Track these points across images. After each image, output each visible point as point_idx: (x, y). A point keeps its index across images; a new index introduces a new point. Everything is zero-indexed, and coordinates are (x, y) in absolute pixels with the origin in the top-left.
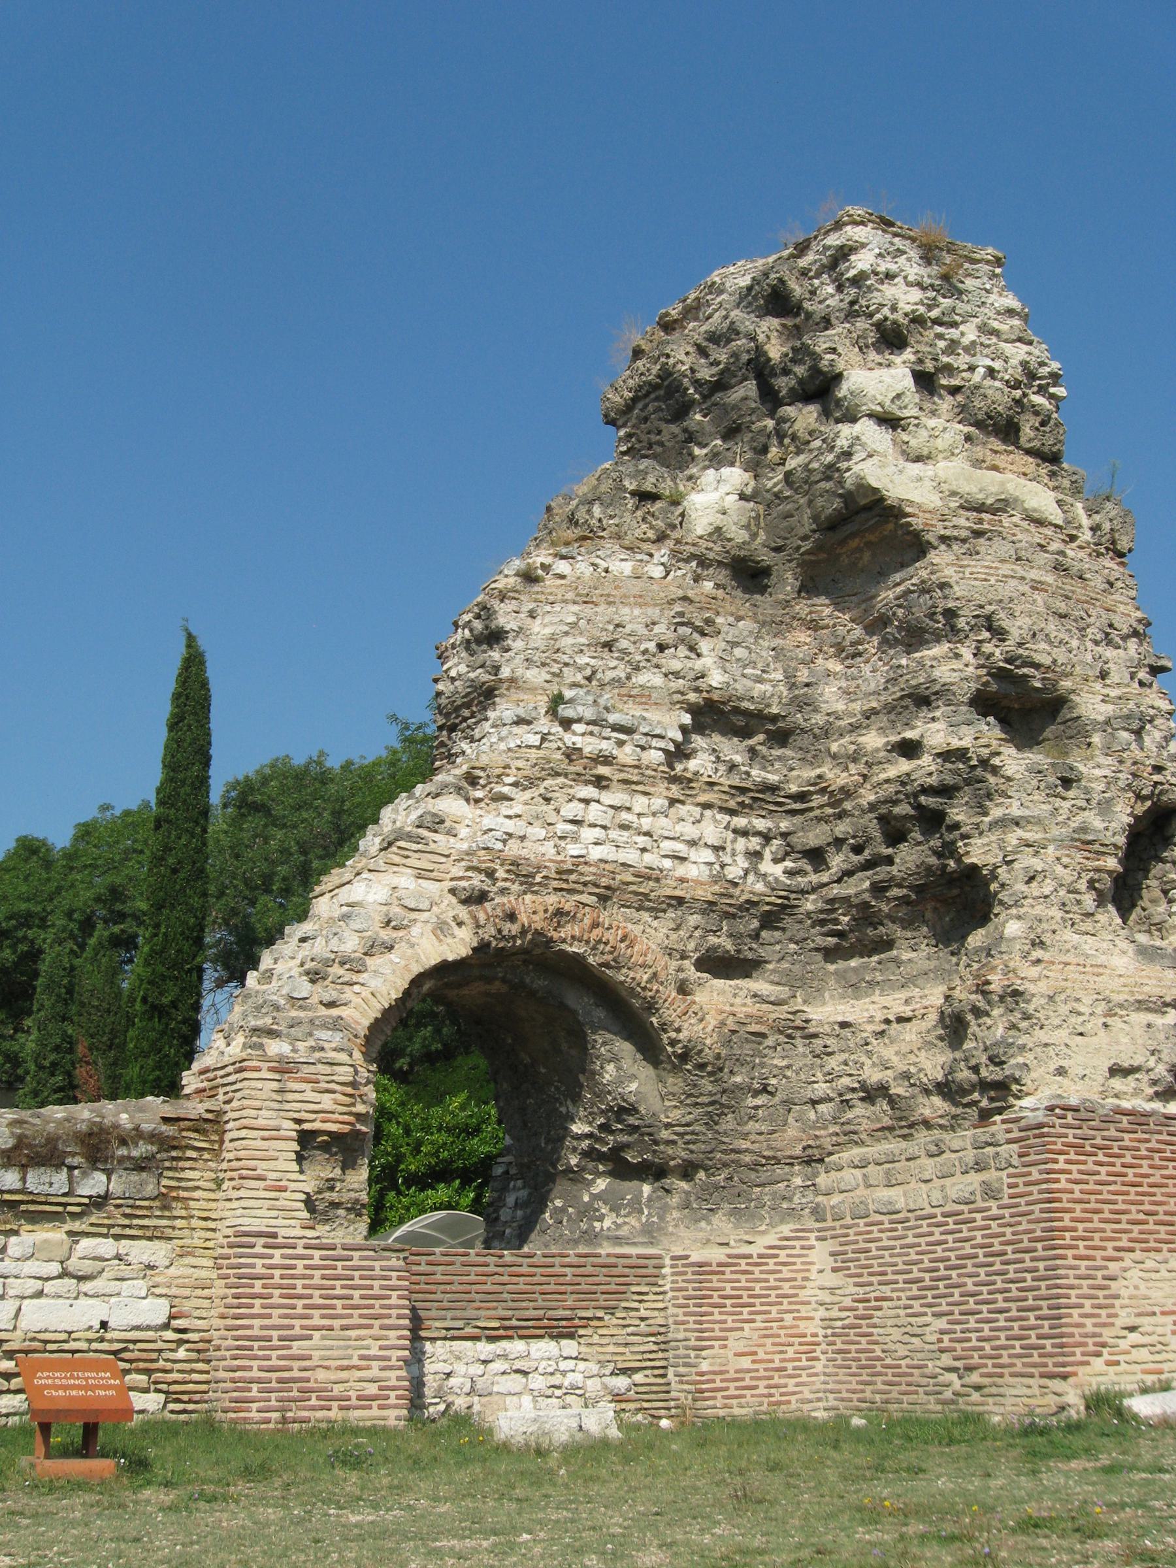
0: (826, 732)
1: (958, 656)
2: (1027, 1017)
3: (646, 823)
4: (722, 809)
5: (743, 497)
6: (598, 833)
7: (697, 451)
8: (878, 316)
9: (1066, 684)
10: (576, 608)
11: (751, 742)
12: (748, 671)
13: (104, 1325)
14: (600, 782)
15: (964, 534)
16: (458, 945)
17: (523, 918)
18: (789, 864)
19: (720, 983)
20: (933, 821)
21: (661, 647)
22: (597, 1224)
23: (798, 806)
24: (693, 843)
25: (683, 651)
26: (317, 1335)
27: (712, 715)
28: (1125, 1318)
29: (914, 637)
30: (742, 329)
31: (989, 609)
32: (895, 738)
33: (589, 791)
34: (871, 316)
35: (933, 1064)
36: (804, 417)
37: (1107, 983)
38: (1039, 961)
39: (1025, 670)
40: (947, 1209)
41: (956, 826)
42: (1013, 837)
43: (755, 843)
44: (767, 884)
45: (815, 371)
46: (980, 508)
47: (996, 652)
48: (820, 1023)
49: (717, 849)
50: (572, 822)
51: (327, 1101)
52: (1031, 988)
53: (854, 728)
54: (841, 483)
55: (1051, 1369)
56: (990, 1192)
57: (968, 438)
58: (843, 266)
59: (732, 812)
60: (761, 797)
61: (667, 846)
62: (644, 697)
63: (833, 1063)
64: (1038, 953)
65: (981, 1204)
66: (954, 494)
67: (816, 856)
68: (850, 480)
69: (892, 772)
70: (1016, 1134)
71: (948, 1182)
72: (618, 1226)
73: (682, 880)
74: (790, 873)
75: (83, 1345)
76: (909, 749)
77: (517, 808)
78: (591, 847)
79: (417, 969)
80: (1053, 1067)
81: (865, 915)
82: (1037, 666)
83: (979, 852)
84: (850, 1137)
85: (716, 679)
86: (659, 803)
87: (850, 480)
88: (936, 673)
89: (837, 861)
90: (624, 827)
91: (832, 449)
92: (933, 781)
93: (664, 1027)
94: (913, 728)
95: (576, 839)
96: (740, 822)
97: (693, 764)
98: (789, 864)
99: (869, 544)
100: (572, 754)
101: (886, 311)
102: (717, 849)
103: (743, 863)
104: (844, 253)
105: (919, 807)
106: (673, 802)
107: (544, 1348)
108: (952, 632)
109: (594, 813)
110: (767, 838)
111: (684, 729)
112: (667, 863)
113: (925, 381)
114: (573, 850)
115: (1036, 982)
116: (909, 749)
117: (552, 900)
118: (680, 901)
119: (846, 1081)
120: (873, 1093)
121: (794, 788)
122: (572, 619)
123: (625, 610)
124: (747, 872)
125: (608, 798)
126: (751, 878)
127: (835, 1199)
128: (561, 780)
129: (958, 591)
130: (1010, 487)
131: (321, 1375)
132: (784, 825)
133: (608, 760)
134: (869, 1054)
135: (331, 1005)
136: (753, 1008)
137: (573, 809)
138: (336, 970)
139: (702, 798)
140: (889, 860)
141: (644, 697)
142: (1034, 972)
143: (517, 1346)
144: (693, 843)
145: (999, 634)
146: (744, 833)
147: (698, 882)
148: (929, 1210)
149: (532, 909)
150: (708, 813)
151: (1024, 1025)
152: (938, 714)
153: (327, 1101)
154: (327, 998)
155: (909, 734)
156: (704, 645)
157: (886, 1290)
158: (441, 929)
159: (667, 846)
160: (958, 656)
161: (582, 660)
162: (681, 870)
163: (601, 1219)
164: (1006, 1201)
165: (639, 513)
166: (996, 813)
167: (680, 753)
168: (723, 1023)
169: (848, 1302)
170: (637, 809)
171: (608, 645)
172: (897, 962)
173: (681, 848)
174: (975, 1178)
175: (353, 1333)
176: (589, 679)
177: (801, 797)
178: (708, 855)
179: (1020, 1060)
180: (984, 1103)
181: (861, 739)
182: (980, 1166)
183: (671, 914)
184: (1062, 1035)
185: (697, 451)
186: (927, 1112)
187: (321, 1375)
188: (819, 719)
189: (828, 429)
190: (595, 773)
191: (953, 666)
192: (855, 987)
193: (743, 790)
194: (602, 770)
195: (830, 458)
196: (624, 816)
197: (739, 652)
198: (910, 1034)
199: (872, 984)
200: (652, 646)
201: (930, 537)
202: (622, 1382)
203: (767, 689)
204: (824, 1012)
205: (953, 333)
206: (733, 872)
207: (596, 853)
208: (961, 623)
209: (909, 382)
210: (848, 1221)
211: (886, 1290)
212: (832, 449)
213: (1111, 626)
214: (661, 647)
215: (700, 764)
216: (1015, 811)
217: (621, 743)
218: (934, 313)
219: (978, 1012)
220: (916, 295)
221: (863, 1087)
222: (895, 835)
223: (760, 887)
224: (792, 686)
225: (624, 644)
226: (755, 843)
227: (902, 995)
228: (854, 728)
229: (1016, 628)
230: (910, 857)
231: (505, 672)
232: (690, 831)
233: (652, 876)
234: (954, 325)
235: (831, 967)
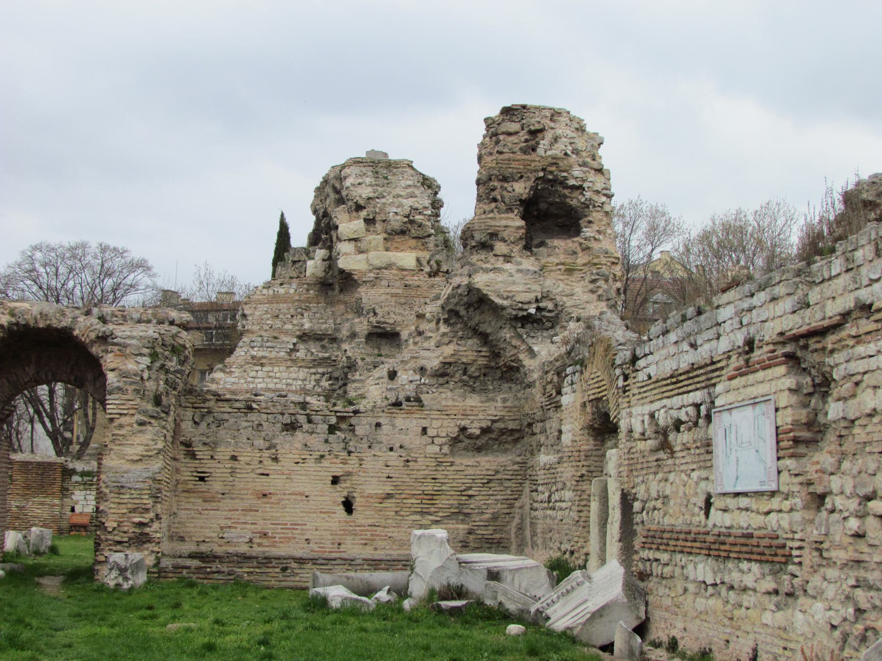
3: (278, 375)
4: (306, 367)
5: (324, 260)
9: (398, 329)
11: (323, 343)
14: (262, 365)
15: (371, 279)
18: (330, 382)
21: (292, 316)
25: (299, 316)
27: (304, 337)
33: (259, 368)
43: (318, 376)
46: (380, 269)
47: (373, 320)
49: (303, 380)
57: (385, 239)
59: (309, 368)
67: (337, 379)
74: (332, 385)
77: (237, 374)
85: (307, 326)
90: (270, 377)
96: (313, 370)
100: (253, 357)
101: (358, 198)
102: (303, 380)
103: (313, 383)
106: (288, 367)
109: (260, 374)
110: (323, 374)
111: (294, 344)
114: (251, 386)
124: (314, 386)
125: (265, 369)
132: (330, 370)
133: (265, 357)
137: (253, 374)
144: (294, 379)
145: (375, 314)
146: (315, 374)
161: (268, 322)
167: (294, 350)
171: (277, 316)
178: (300, 382)
193: (314, 360)
194: (264, 361)
196: (271, 374)
197: (317, 315)
200: (289, 316)
201: (359, 282)
203: (328, 326)
205: (383, 200)
208: (364, 312)
214: (292, 316)
215: (301, 354)
218: (376, 195)
220: (370, 189)
224: (335, 324)
225: (281, 316)
226: (318, 376)
231: (246, 328)
232: (294, 376)
234: (384, 197)
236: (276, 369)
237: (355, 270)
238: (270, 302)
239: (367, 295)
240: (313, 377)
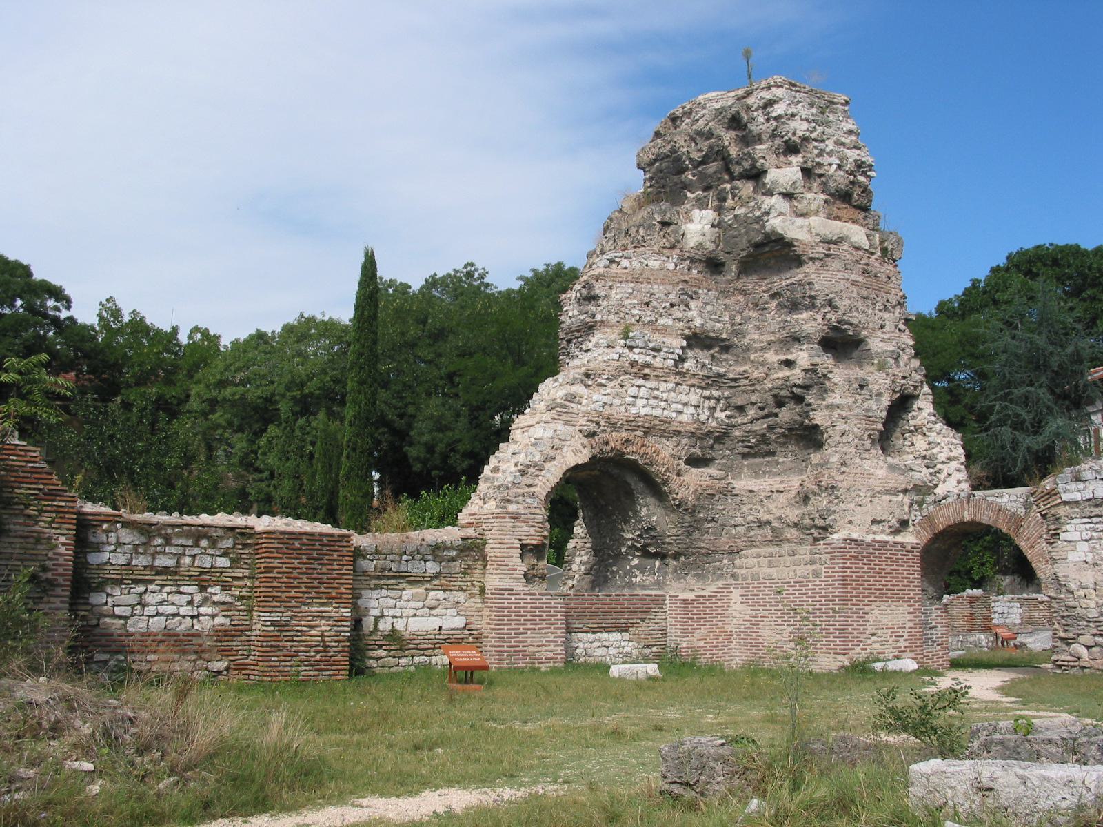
0: (748, 349)
1: (815, 319)
2: (837, 498)
3: (665, 395)
5: (713, 226)
6: (644, 402)
7: (689, 195)
8: (786, 138)
9: (864, 333)
10: (632, 285)
11: (712, 352)
12: (713, 317)
13: (440, 628)
14: (646, 377)
15: (821, 256)
16: (583, 457)
17: (612, 444)
18: (728, 413)
19: (695, 470)
20: (799, 400)
21: (672, 305)
22: (634, 580)
23: (733, 384)
24: (685, 404)
25: (682, 307)
26: (529, 632)
27: (697, 340)
28: (870, 630)
29: (794, 307)
30: (715, 133)
31: (831, 296)
32: (783, 358)
33: (640, 382)
34: (783, 137)
35: (793, 515)
36: (747, 188)
37: (873, 482)
38: (844, 472)
39: (846, 326)
40: (798, 579)
41: (810, 405)
42: (836, 413)
44: (718, 423)
45: (753, 166)
46: (830, 242)
47: (833, 317)
48: (740, 490)
49: (696, 407)
50: (634, 397)
51: (532, 531)
52: (840, 484)
53: (763, 349)
54: (763, 227)
55: (838, 651)
56: (816, 574)
57: (826, 201)
58: (769, 109)
59: (703, 388)
60: (716, 380)
61: (674, 406)
62: (664, 331)
63: (745, 509)
64: (843, 469)
65: (811, 579)
66: (817, 235)
67: (741, 409)
68: (768, 229)
69: (780, 375)
70: (829, 550)
71: (797, 568)
72: (644, 581)
73: (680, 423)
74: (729, 417)
75: (432, 637)
76: (789, 364)
77: (608, 390)
78: (642, 409)
79: (565, 468)
80: (847, 520)
81: (764, 439)
82: (851, 324)
83: (819, 418)
84: (751, 543)
85: (698, 322)
86: (671, 385)
87: (768, 229)
88: (804, 327)
89: (752, 412)
91: (760, 209)
92: (799, 382)
93: (670, 492)
94: (792, 353)
95: (634, 404)
96: (707, 393)
97: (686, 365)
98: (728, 413)
99: (775, 257)
100: (633, 363)
102: (696, 407)
103: (707, 413)
104: (771, 103)
105: (792, 392)
106: (677, 384)
107: (615, 636)
108: (812, 306)
110: (718, 400)
111: (682, 348)
112: (674, 415)
113: (807, 172)
114: (634, 410)
116: (789, 364)
117: (624, 435)
118: (679, 432)
119: (751, 518)
120: (762, 524)
121: (732, 376)
122: (630, 291)
123: (656, 287)
124: (709, 417)
125: (650, 384)
126: (710, 420)
127: (744, 571)
128: (628, 376)
129: (817, 287)
130: (845, 230)
131: (531, 649)
132: (726, 394)
133: (649, 366)
134: (763, 506)
135: (530, 486)
136: (710, 482)
137: (633, 391)
138: (532, 470)
139: (689, 383)
140: (776, 415)
141: (664, 331)
142: (841, 477)
143: (604, 635)
144: (685, 404)
145: (835, 308)
146: (708, 398)
147: (687, 424)
148: (788, 580)
149: (616, 439)
150: (692, 389)
151: (836, 501)
152: (804, 347)
153: (532, 531)
154: (528, 483)
155: (789, 357)
156: (692, 304)
157: (766, 613)
158: (575, 452)
159: (674, 406)
160: (815, 319)
162: (680, 418)
163: (636, 577)
164: (823, 579)
165: (662, 233)
166: (829, 401)
167: (682, 359)
168: (696, 490)
169: (747, 617)
170: (661, 389)
171: (647, 304)
172: (777, 463)
173: (680, 406)
174: (810, 568)
175: (543, 631)
176: (638, 321)
177: (735, 380)
178: (692, 410)
179: (833, 517)
180: (816, 535)
181: (766, 355)
182: (812, 563)
183: (674, 439)
184: (852, 505)
185: (689, 195)
186: (789, 536)
187: (531, 649)
188: (745, 341)
189: (760, 198)
190: (641, 371)
191: (810, 323)
192: (757, 474)
193: (708, 377)
194: (647, 371)
195: (758, 213)
196: (656, 392)
197: (709, 308)
198: (782, 499)
199: (764, 473)
200: (668, 305)
201: (804, 258)
202: (648, 651)
203: (721, 327)
205: (822, 146)
206: (703, 418)
207: (643, 411)
208: (818, 303)
209: (799, 174)
210: (749, 581)
211: (766, 613)
212: (760, 209)
213: (888, 301)
214: (672, 305)
216: (837, 401)
217: (655, 357)
218: (814, 135)
219: (814, 494)
220: (805, 126)
221: (759, 521)
222: (780, 403)
223: (714, 424)
224: (733, 325)
225: (655, 303)
227: (778, 479)
228: (763, 349)
229: (843, 304)
230: (786, 415)
231: (598, 317)
232: (684, 398)
233: (667, 421)
234: (823, 141)
235: (745, 463)
236: (663, 386)
237: (797, 240)
238: (637, 281)
239: (822, 279)
240: (707, 404)
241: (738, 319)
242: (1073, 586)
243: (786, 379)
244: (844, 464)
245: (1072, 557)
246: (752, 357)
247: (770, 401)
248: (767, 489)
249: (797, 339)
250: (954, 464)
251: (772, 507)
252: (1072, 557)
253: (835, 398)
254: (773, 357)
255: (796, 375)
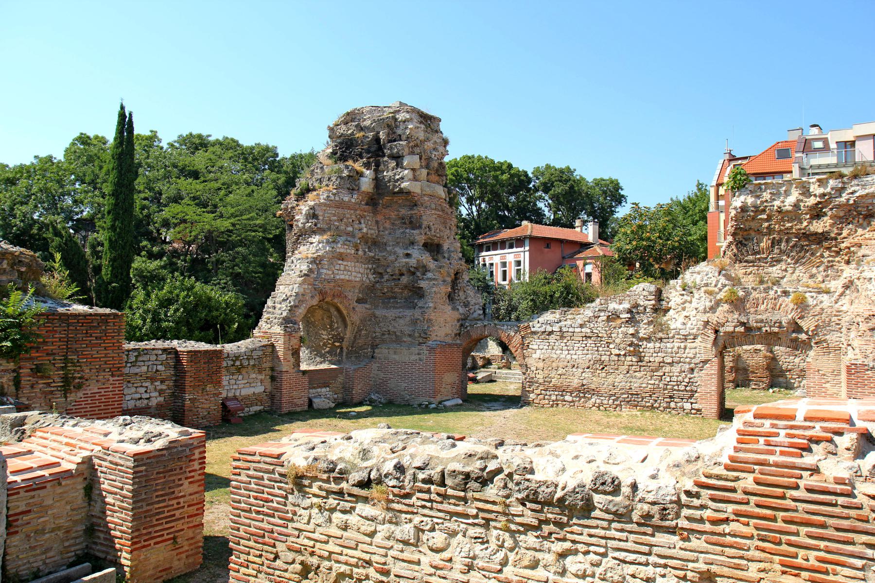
20: (414, 274)
32: (406, 252)
33: (340, 262)
36: (393, 164)
56: (420, 360)
76: (408, 255)
83: (423, 284)
84: (383, 341)
85: (365, 230)
107: (324, 390)
115: (433, 316)
116: (408, 255)
143: (319, 390)
156: (362, 221)
161: (336, 223)
174: (417, 357)
182: (419, 354)
191: (420, 237)
198: (401, 321)
204: (379, 312)
222: (402, 275)
230: (405, 280)
241: (381, 229)
242: (533, 368)
243: (407, 263)
244: (435, 308)
245: (534, 356)
246: (388, 249)
247: (397, 272)
248: (397, 318)
249: (412, 243)
250: (477, 307)
251: (396, 325)
252: (534, 356)
253: (429, 275)
254: (401, 252)
255: (413, 262)
